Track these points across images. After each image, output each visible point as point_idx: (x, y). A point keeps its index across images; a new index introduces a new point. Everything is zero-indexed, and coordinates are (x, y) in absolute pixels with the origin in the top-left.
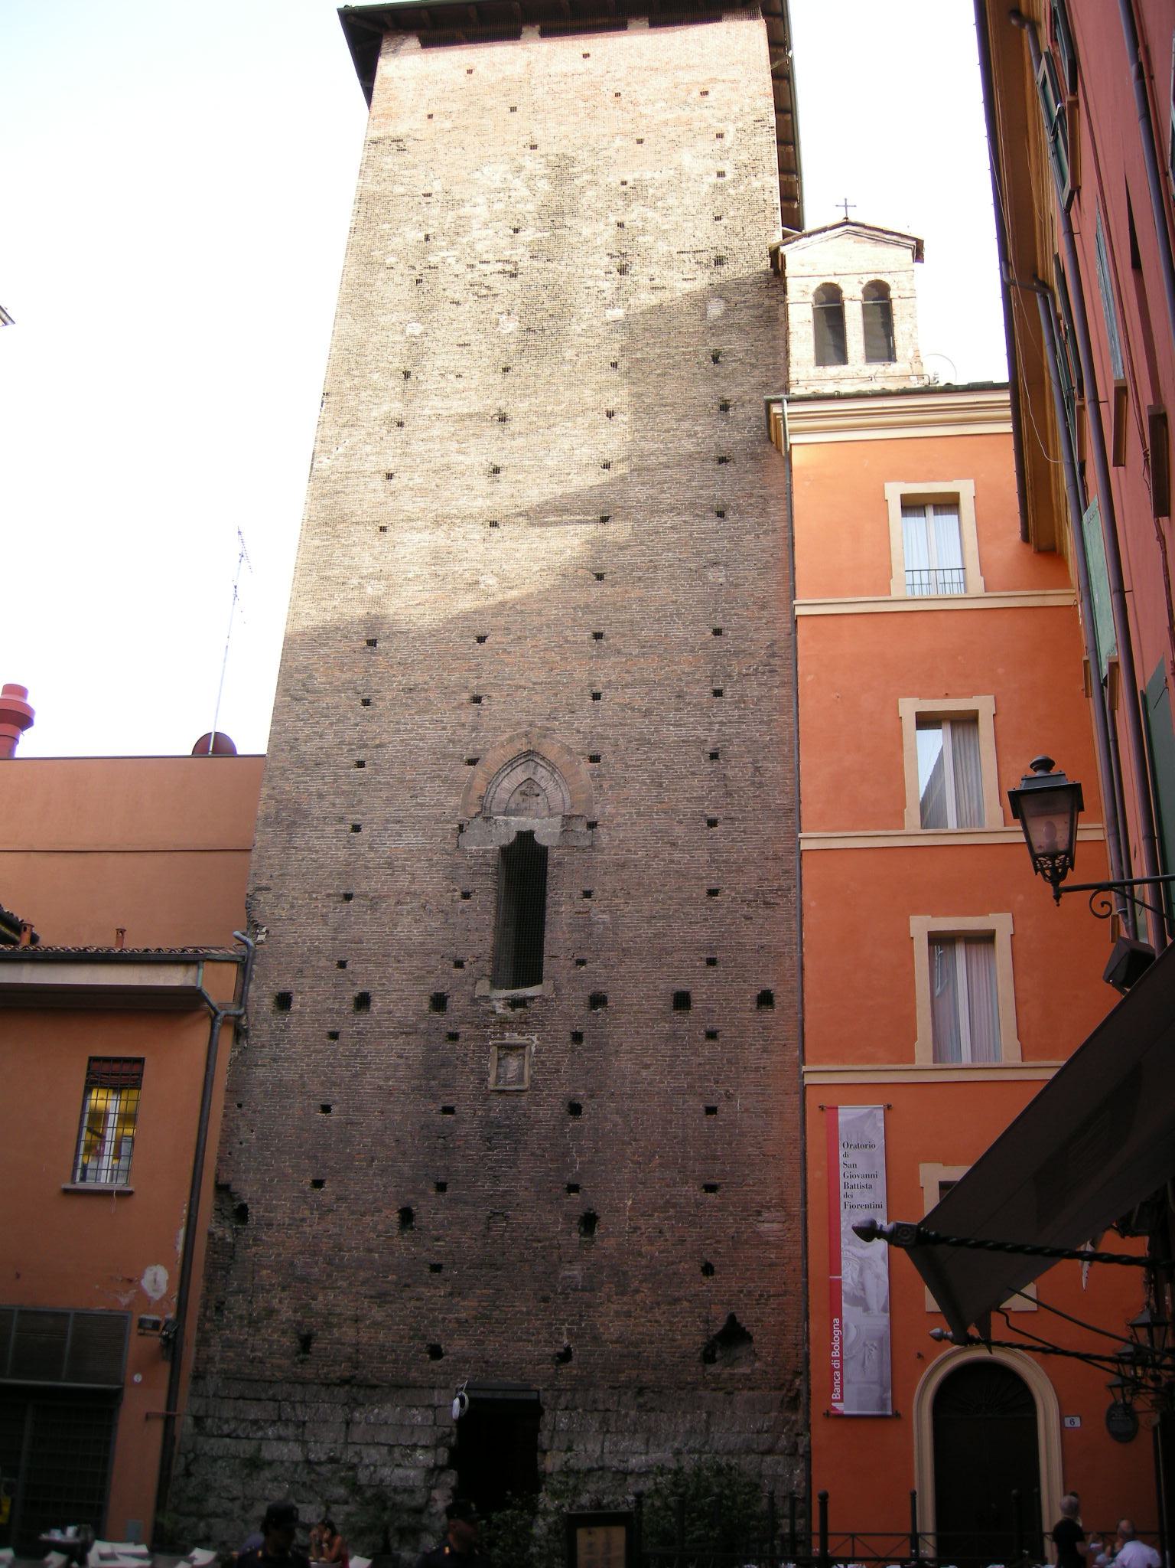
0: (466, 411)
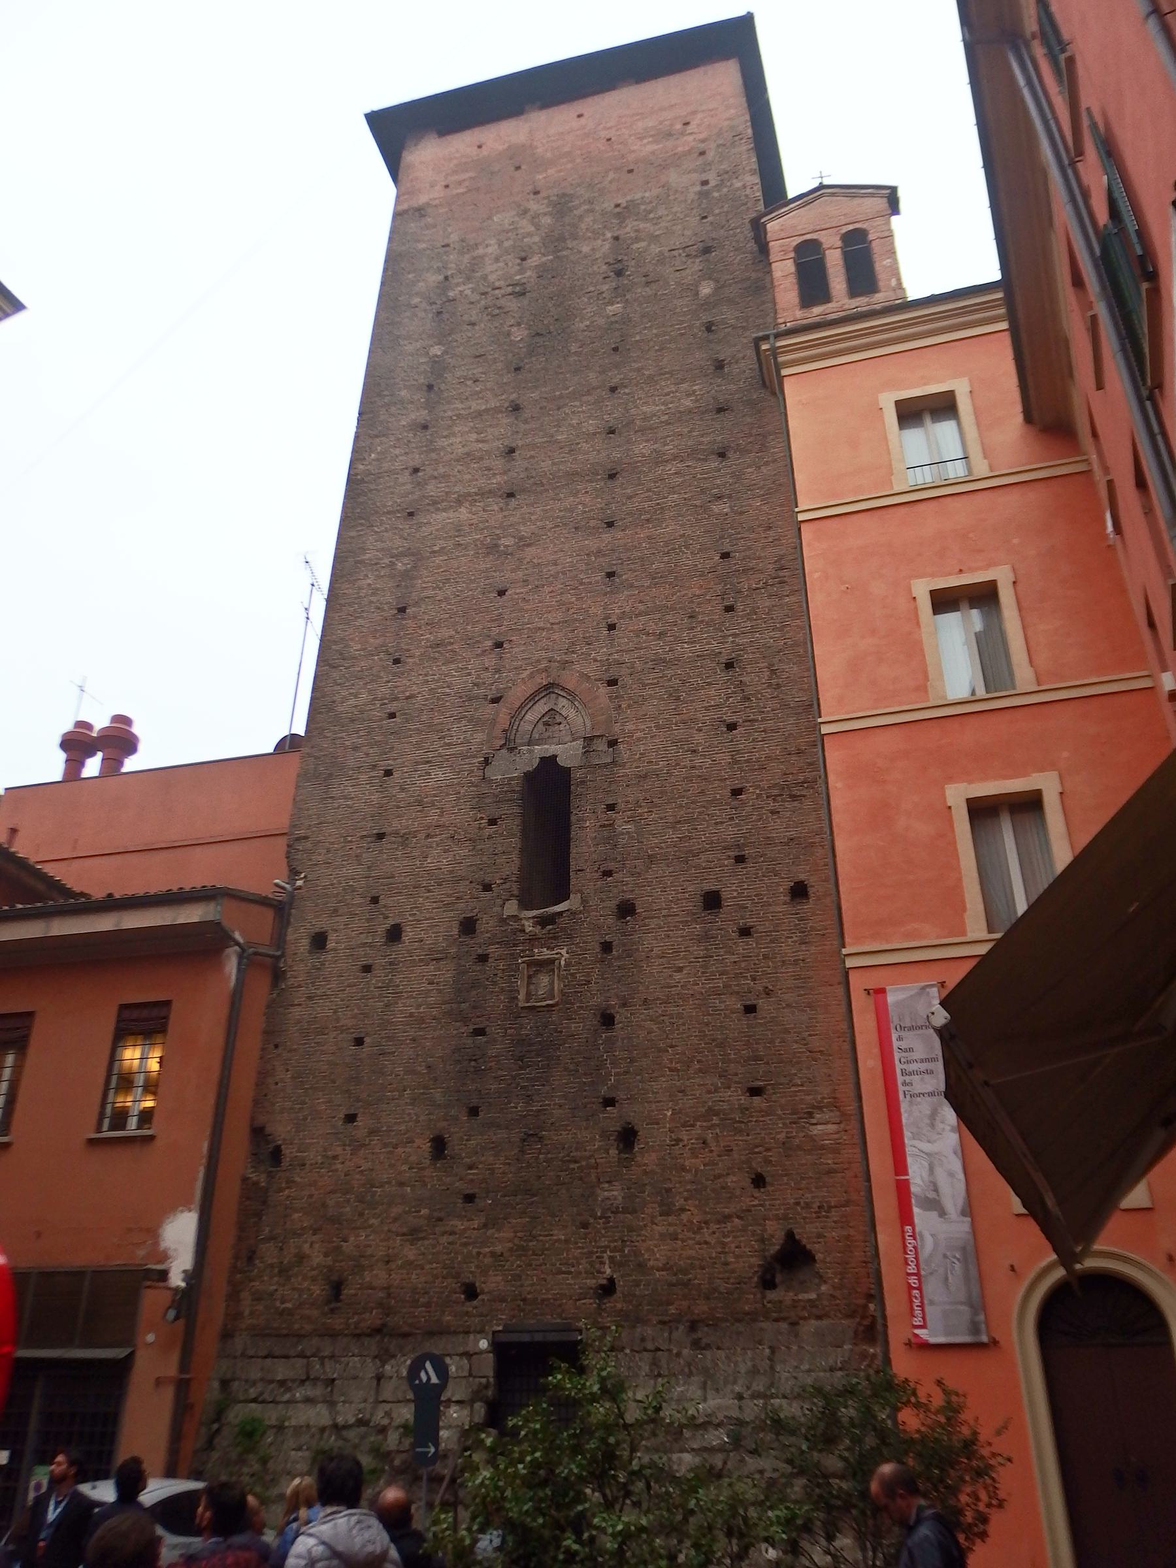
0: (484, 407)
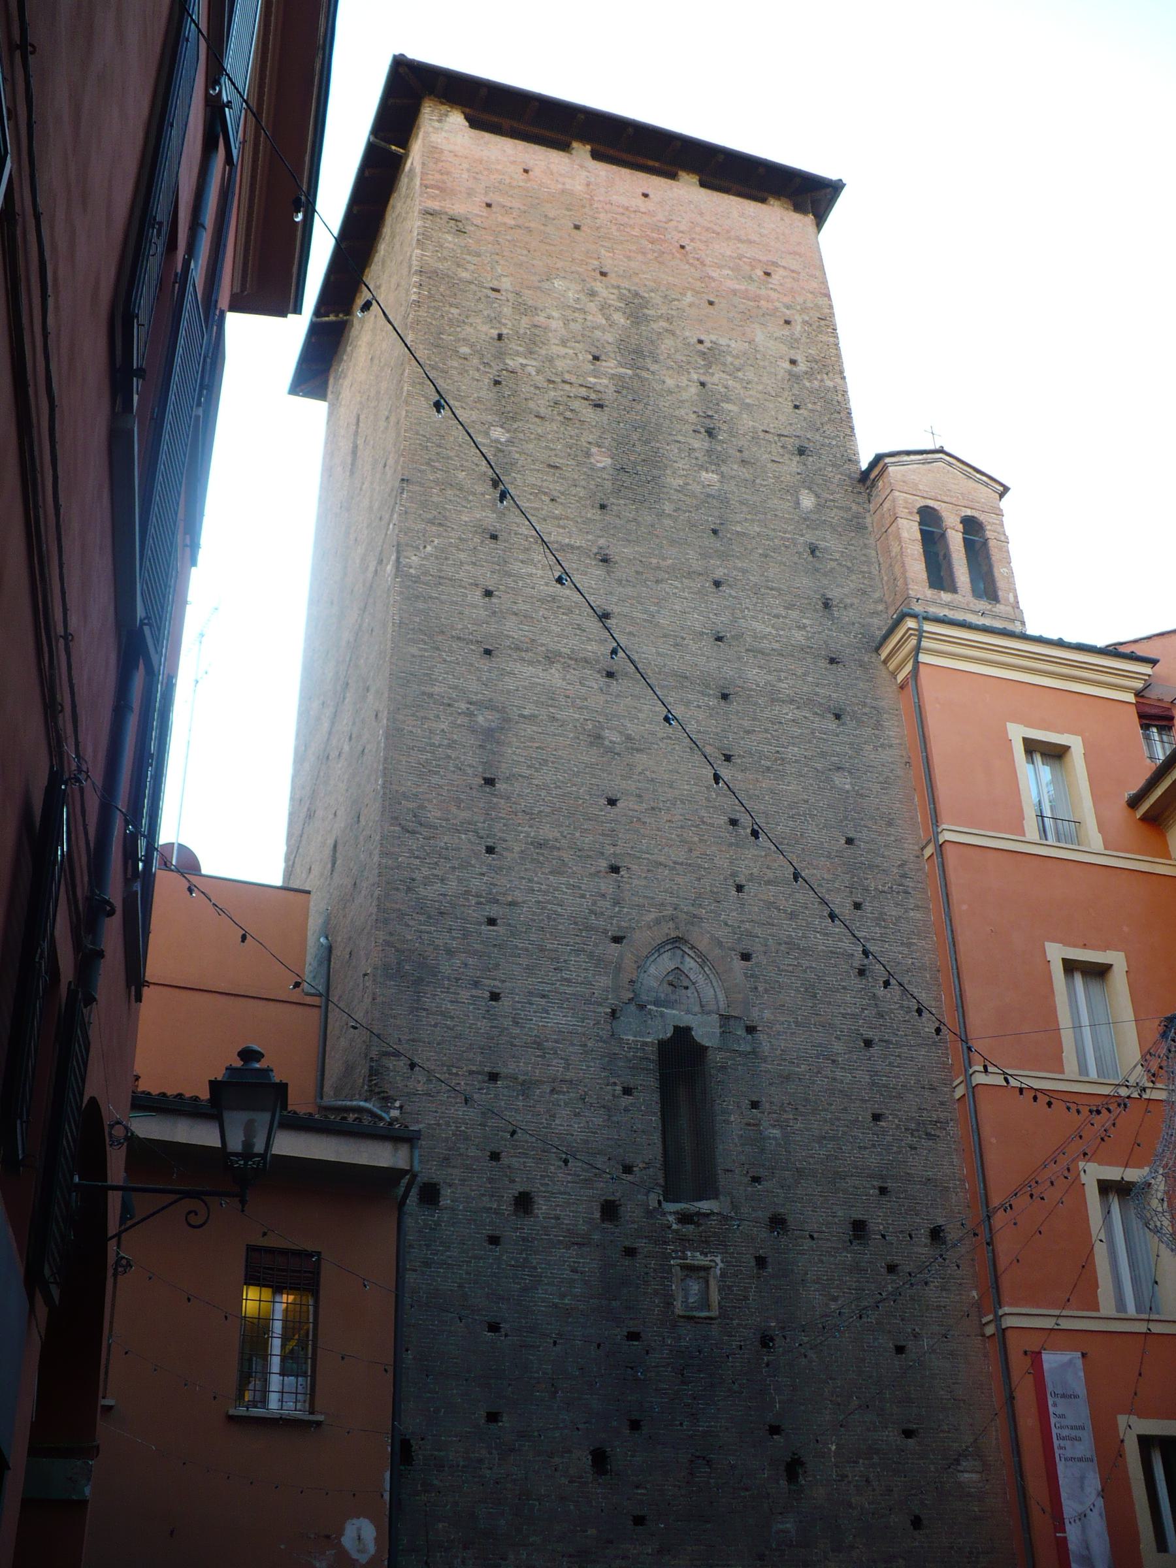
0: (567, 541)
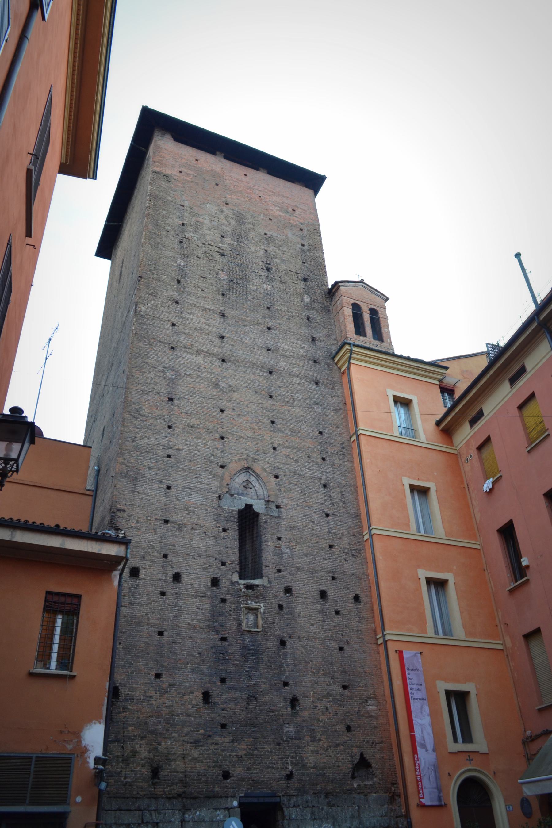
0: (207, 307)
